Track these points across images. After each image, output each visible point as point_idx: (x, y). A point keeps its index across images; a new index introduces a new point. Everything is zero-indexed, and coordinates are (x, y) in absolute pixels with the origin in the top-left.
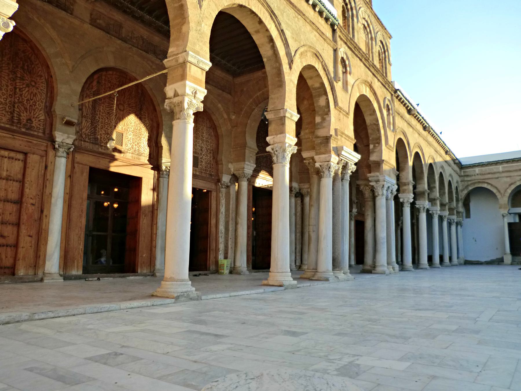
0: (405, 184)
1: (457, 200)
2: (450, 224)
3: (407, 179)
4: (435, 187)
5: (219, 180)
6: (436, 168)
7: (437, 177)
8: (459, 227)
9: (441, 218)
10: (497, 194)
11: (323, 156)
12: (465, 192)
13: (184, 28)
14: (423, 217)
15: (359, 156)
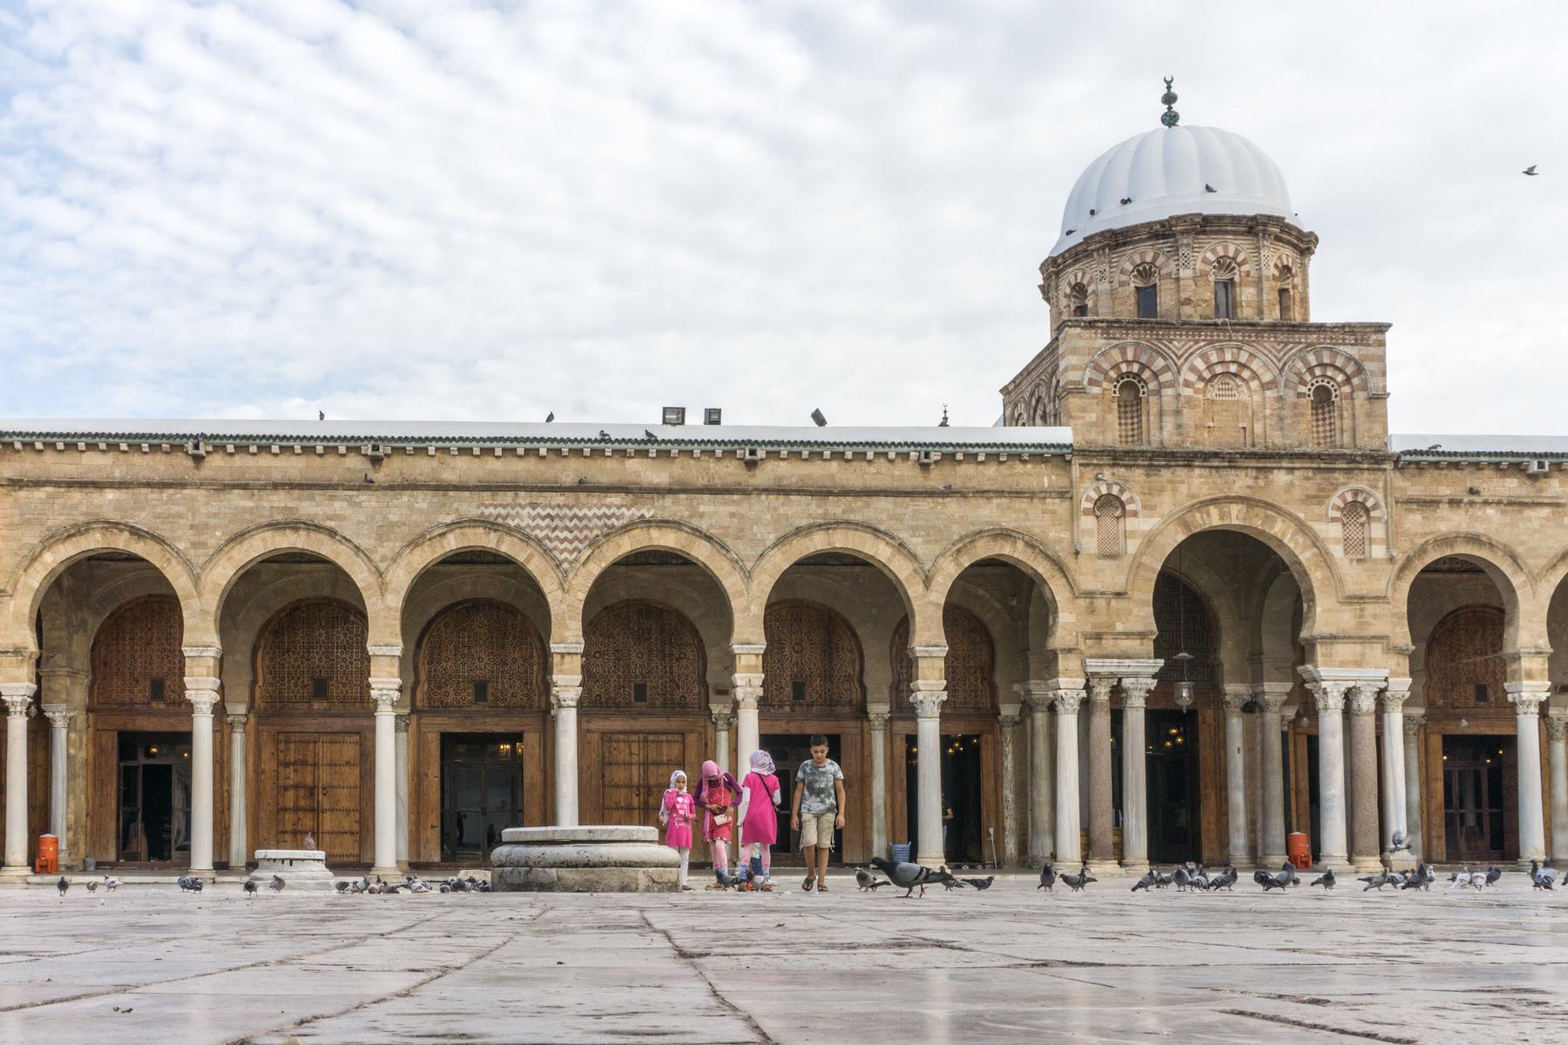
3: (1515, 643)
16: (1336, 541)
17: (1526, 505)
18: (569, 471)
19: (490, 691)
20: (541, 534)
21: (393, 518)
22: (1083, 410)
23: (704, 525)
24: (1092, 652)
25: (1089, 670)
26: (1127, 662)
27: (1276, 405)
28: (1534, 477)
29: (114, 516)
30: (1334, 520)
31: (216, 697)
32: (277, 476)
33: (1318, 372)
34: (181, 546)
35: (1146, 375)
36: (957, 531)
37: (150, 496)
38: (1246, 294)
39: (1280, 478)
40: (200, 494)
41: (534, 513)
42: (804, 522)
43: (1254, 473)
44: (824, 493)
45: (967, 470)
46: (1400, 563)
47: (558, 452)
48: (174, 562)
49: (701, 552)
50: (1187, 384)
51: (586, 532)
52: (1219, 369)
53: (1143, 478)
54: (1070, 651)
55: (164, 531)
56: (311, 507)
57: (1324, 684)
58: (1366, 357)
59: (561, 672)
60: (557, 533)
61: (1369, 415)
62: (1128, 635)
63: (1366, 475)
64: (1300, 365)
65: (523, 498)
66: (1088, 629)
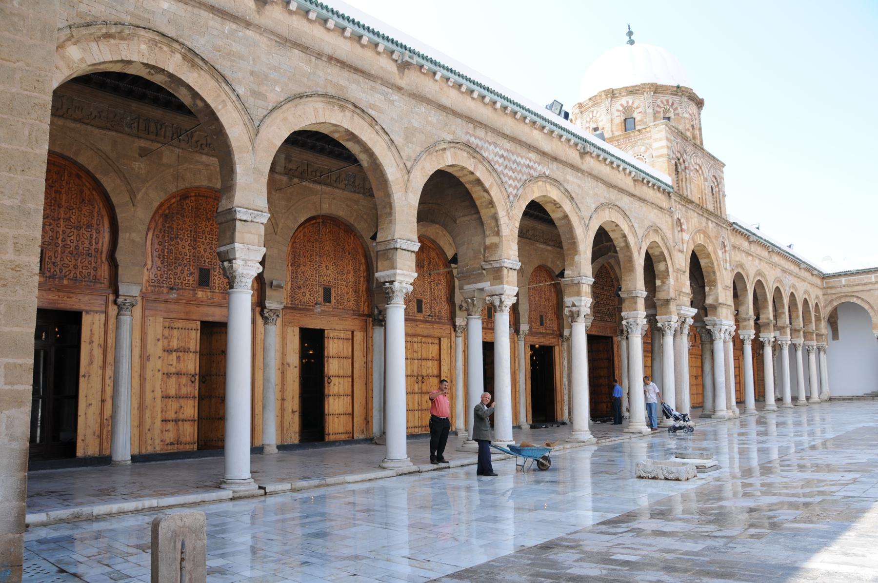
0: (745, 320)
1: (818, 319)
2: (807, 352)
4: (784, 313)
5: (561, 335)
6: (785, 290)
7: (786, 301)
8: (822, 353)
9: (794, 348)
10: (870, 311)
11: (664, 317)
12: (829, 309)
13: (576, 258)
14: (768, 351)
15: (695, 311)
17: (747, 253)
18: (508, 125)
19: (333, 294)
20: (500, 169)
21: (416, 124)
23: (569, 188)
25: (682, 312)
28: (750, 242)
29: (171, 32)
31: (257, 269)
32: (328, 50)
34: (241, 91)
35: (681, 160)
36: (647, 224)
37: (211, 23)
39: (711, 225)
40: (263, 41)
41: (495, 151)
42: (603, 201)
44: (610, 185)
45: (645, 188)
47: (505, 108)
48: (230, 106)
49: (567, 207)
51: (520, 175)
55: (223, 66)
56: (358, 90)
59: (508, 283)
60: (506, 171)
65: (490, 137)
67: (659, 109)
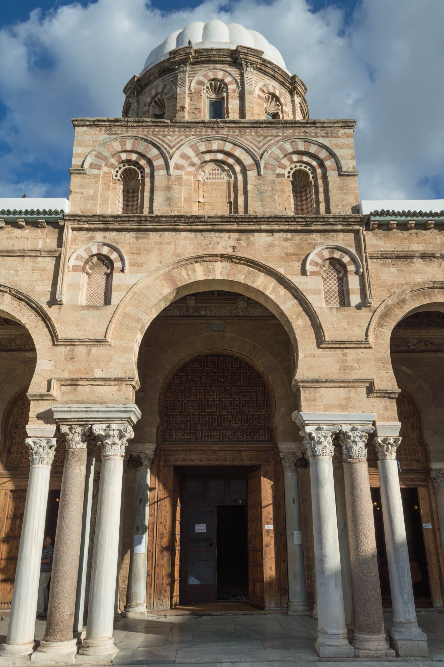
16: (316, 292)
22: (81, 187)
24: (67, 398)
26: (95, 407)
27: (257, 182)
30: (314, 273)
33: (295, 158)
35: (142, 162)
38: (233, 104)
39: (261, 239)
43: (235, 235)
46: (379, 312)
50: (178, 167)
52: (208, 157)
53: (133, 240)
54: (41, 397)
57: (308, 429)
58: (337, 146)
61: (341, 189)
62: (105, 380)
63: (341, 235)
64: (278, 152)
66: (66, 375)
67: (146, 108)
